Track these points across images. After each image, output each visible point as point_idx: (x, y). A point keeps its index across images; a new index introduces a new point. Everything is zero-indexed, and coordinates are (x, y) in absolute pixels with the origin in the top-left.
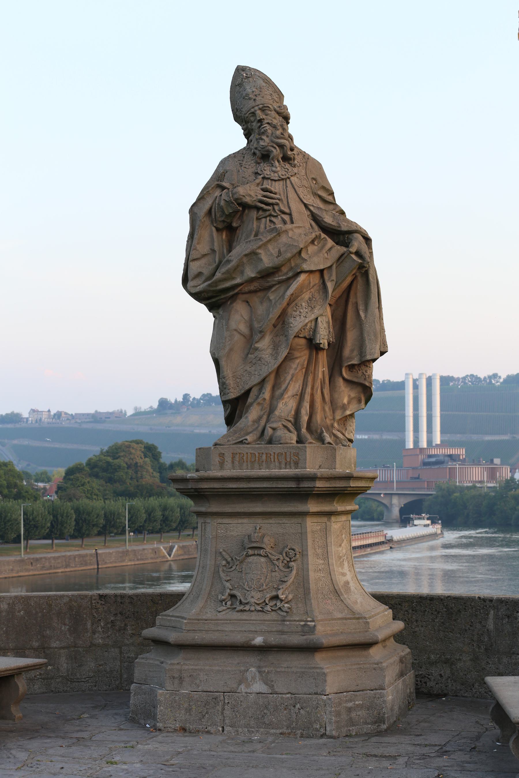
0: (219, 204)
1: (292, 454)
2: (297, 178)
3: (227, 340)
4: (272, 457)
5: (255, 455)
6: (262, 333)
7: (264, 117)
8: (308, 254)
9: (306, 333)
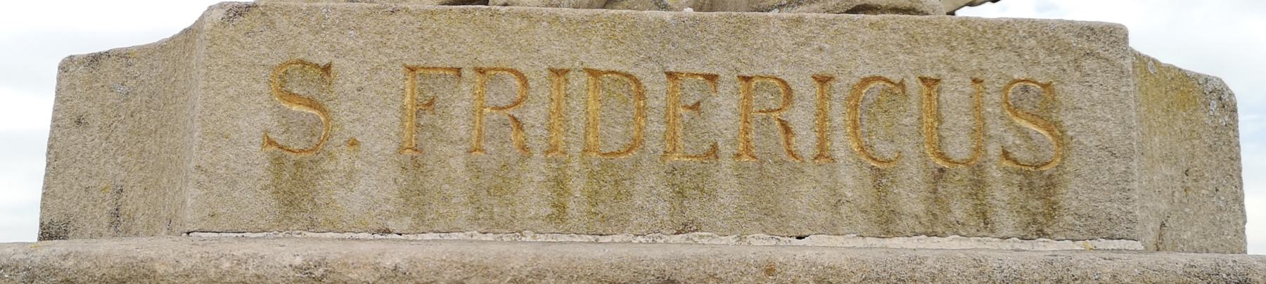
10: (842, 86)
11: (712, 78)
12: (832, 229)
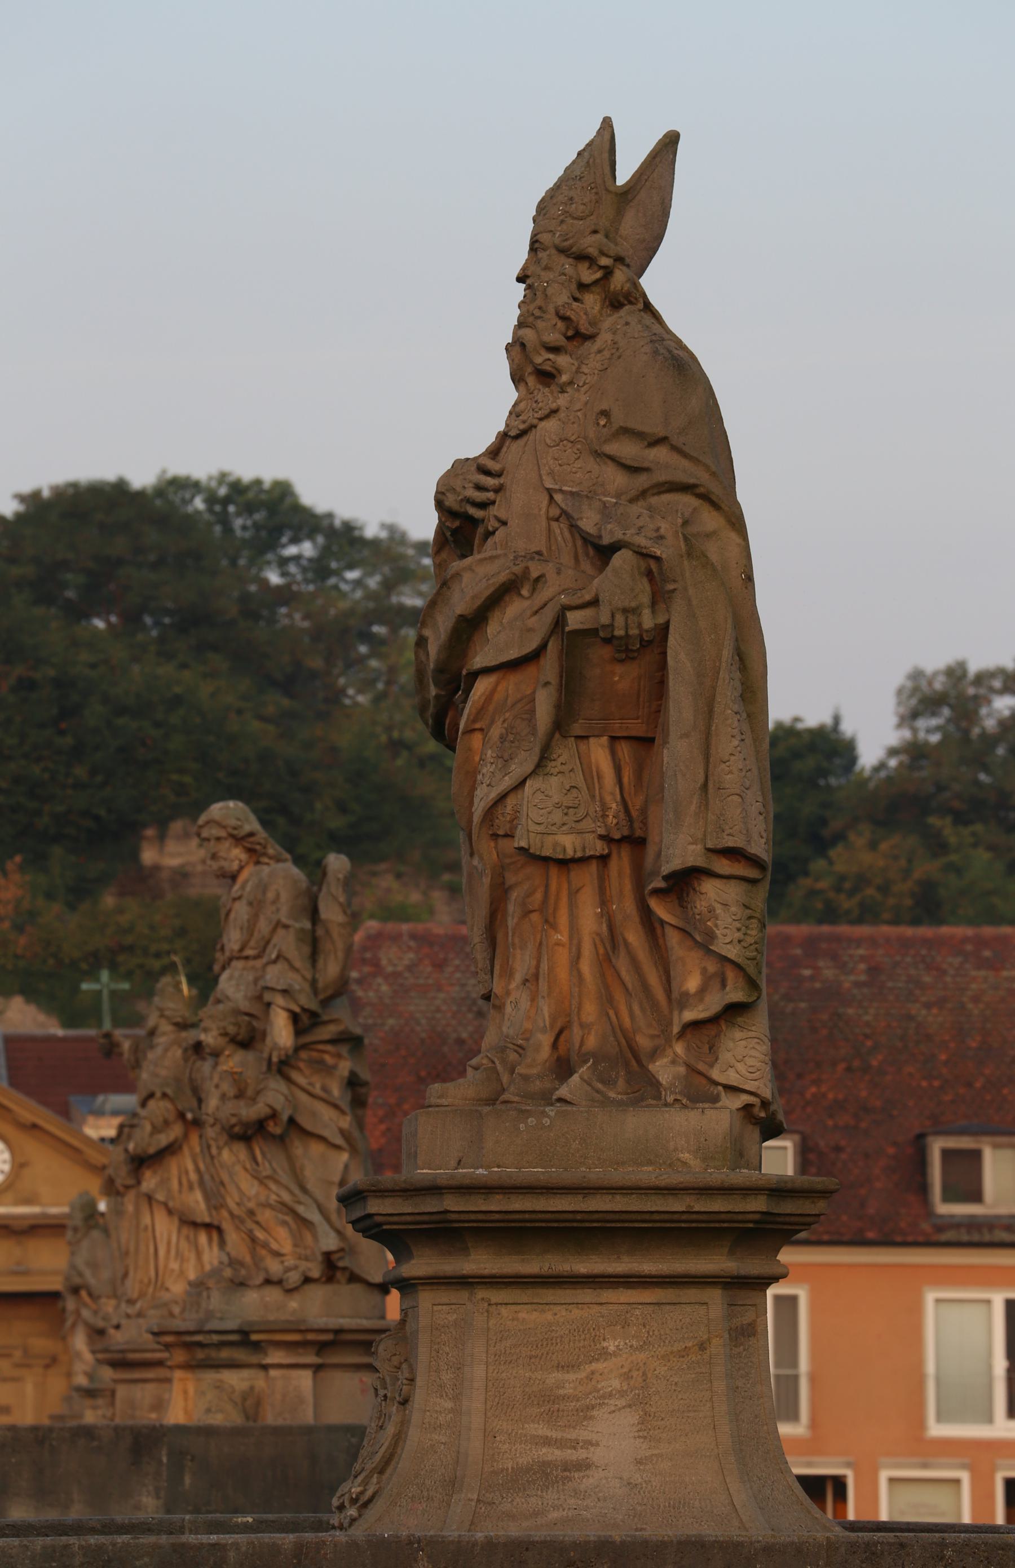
2: (560, 420)
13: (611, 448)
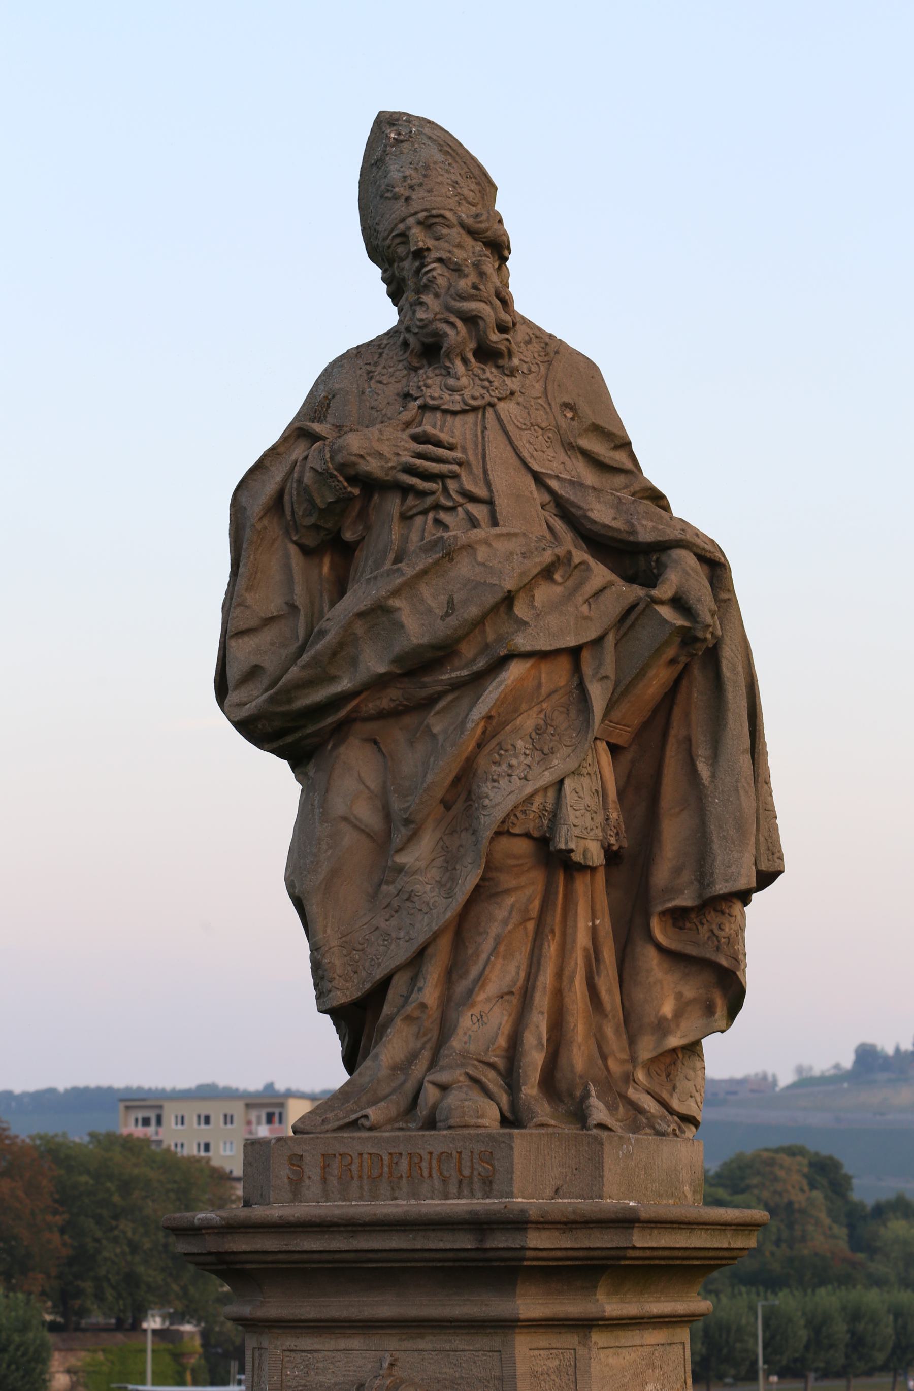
0: (300, 481)
1: (476, 1156)
2: (518, 404)
3: (324, 847)
4: (424, 1164)
5: (382, 1160)
6: (413, 826)
7: (430, 243)
8: (533, 607)
9: (530, 823)
10: (435, 1156)
11: (401, 1154)
12: (432, 1198)
13: (585, 443)
